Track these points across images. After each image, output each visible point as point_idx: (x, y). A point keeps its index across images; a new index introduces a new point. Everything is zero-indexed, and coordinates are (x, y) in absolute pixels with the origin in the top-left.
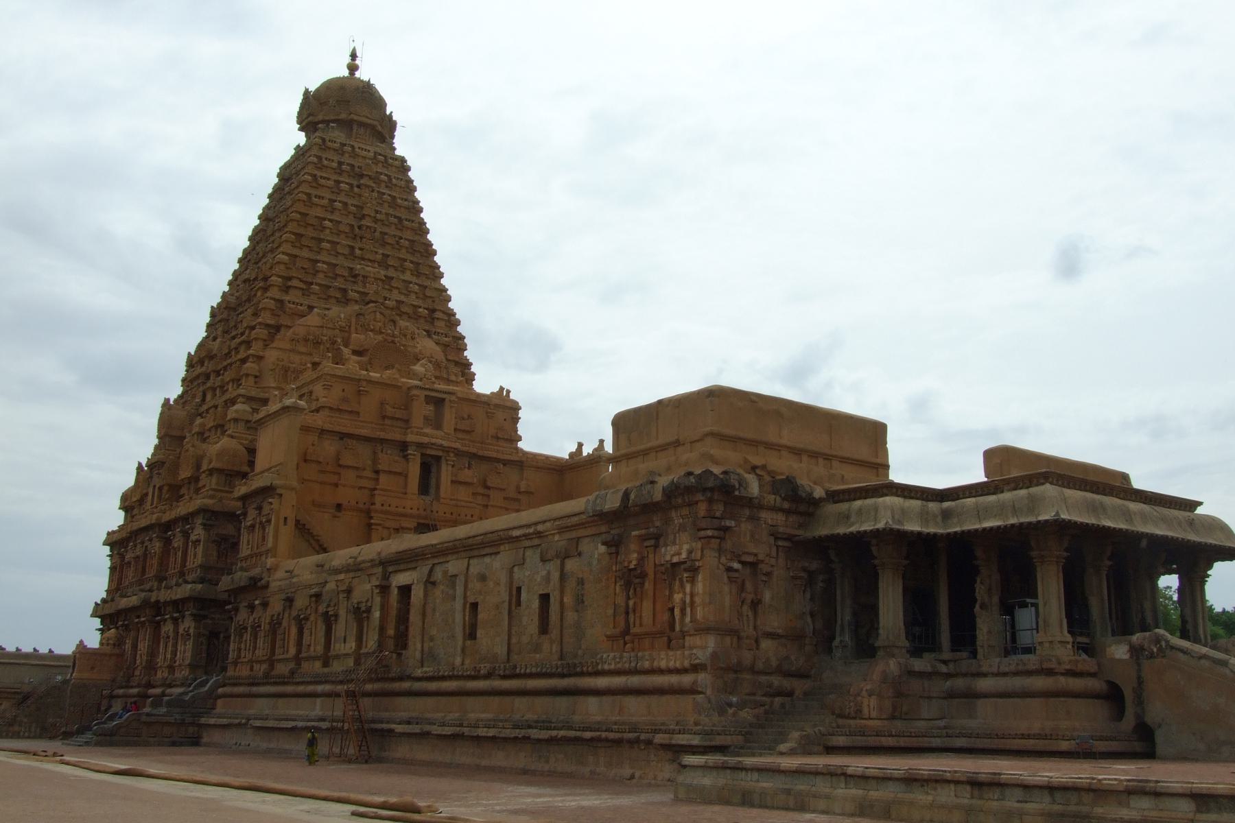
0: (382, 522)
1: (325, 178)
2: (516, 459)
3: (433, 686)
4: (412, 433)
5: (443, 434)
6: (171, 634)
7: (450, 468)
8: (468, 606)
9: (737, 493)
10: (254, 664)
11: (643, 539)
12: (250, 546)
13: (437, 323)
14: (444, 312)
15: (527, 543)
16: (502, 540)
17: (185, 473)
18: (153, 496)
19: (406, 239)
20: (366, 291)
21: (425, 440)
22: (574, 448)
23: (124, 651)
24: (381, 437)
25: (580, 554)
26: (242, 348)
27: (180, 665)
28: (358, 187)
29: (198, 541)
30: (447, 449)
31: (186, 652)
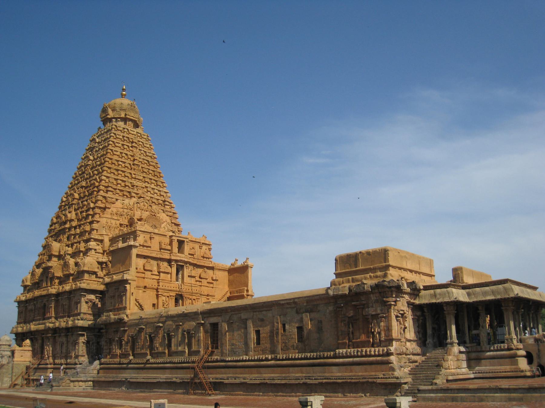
0: (162, 294)
1: (117, 143)
3: (240, 364)
5: (184, 256)
6: (65, 342)
7: (187, 270)
13: (166, 206)
15: (288, 306)
21: (179, 258)
22: (233, 262)
24: (161, 257)
28: (132, 147)
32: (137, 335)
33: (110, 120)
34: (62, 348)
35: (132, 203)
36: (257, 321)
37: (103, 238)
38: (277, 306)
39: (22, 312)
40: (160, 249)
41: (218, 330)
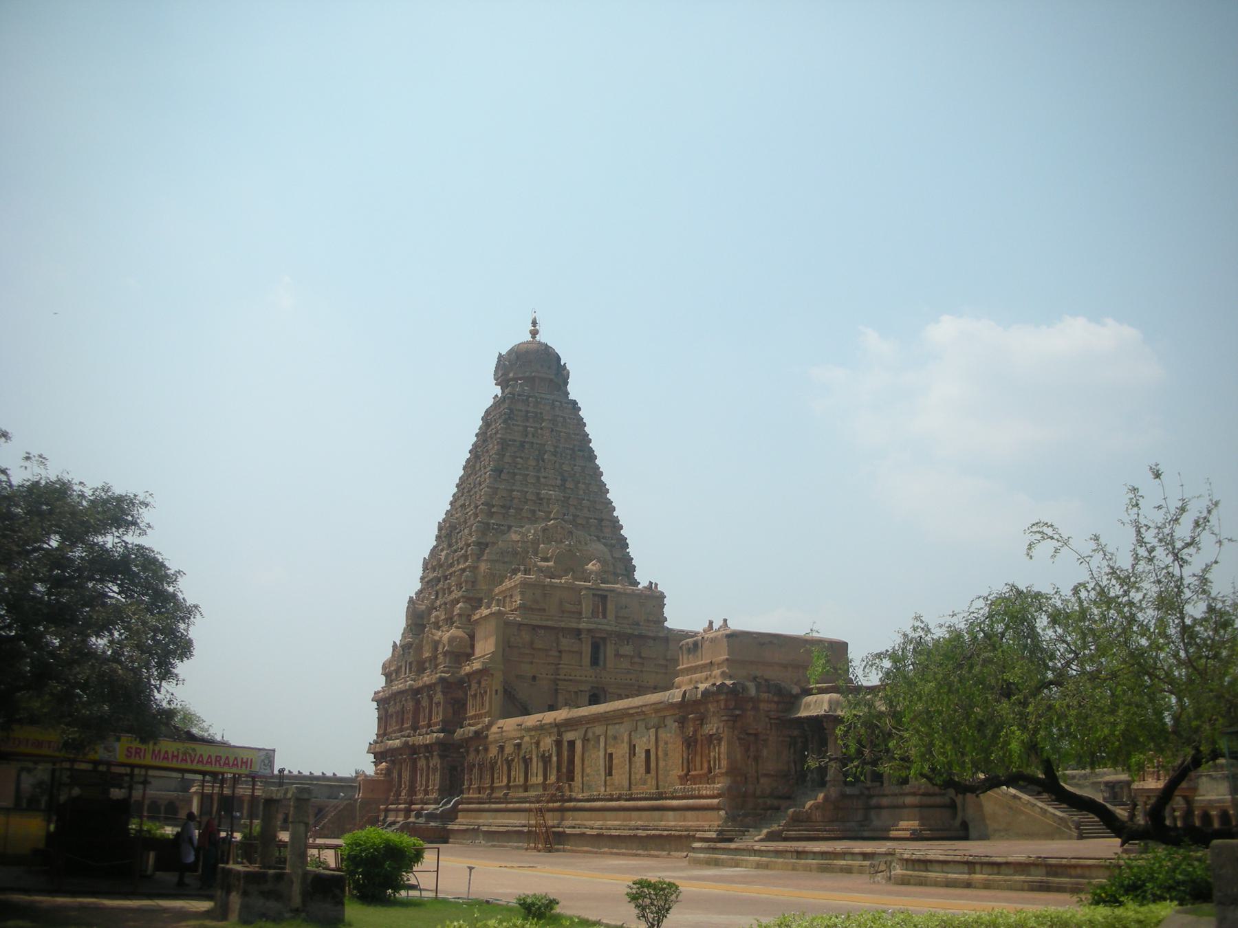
2: (661, 635)
3: (588, 804)
9: (741, 695)
11: (694, 720)
14: (610, 521)
15: (638, 718)
17: (426, 655)
18: (406, 669)
20: (549, 510)
21: (592, 626)
25: (665, 726)
26: (462, 560)
27: (432, 789)
28: (541, 429)
29: (438, 704)
31: (435, 781)
32: (497, 758)
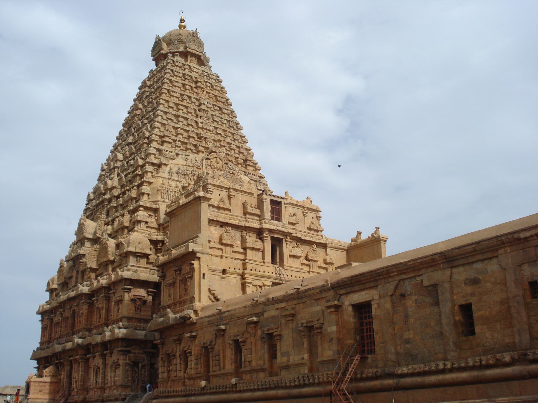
0: (252, 281)
1: (176, 82)
2: (322, 241)
3: (433, 379)
4: (265, 222)
6: (101, 366)
8: (456, 308)
10: (186, 380)
12: (172, 297)
13: (249, 168)
16: (503, 243)
19: (225, 119)
22: (354, 236)
23: (61, 380)
24: (247, 225)
28: (196, 88)
30: (286, 234)
32: (213, 343)
33: (165, 56)
34: (96, 376)
35: (199, 160)
36: (463, 285)
37: (157, 206)
38: (510, 246)
39: (46, 328)
40: (245, 213)
41: (370, 317)
